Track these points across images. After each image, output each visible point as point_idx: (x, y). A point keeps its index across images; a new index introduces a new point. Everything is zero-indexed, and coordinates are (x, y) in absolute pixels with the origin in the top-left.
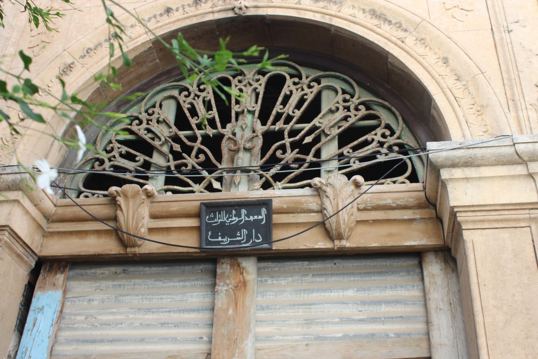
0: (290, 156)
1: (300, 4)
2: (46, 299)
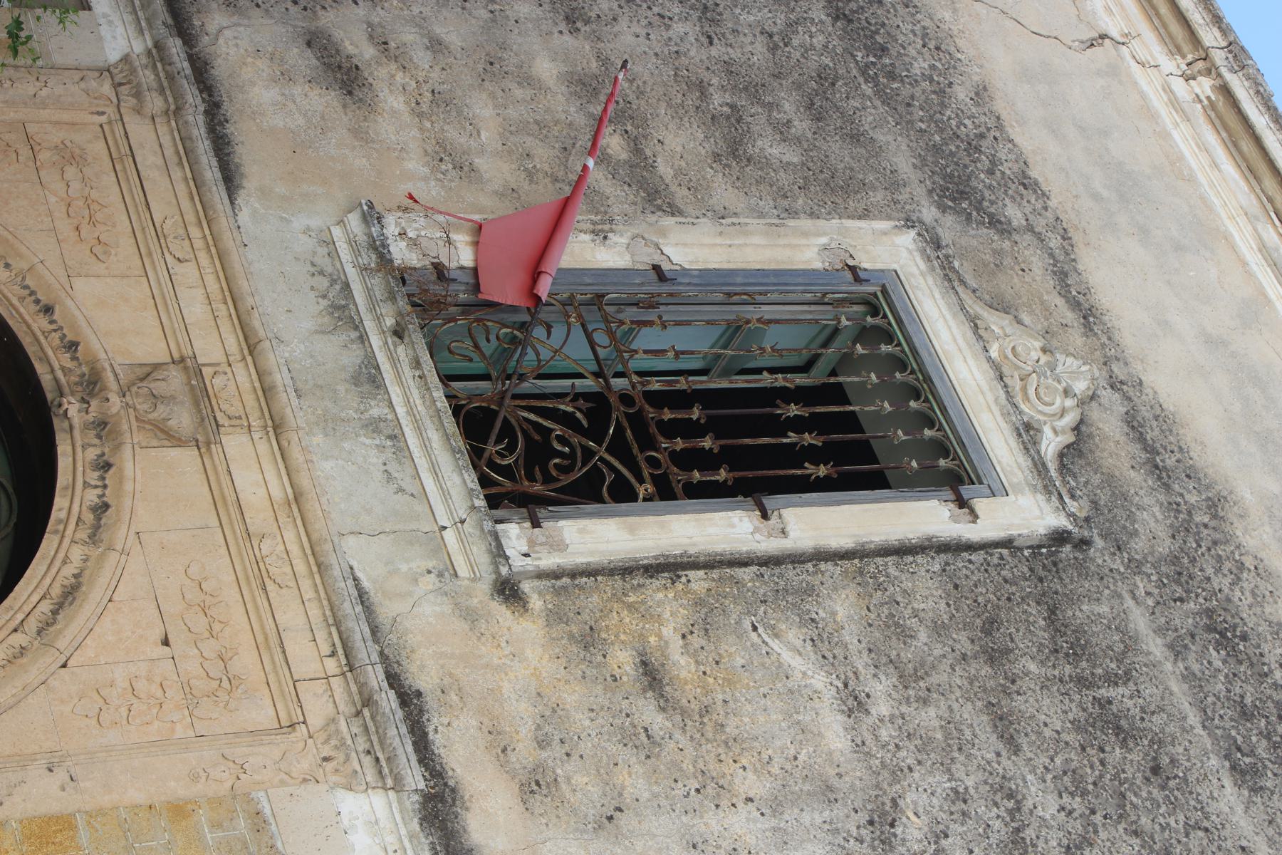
1: (84, 488)
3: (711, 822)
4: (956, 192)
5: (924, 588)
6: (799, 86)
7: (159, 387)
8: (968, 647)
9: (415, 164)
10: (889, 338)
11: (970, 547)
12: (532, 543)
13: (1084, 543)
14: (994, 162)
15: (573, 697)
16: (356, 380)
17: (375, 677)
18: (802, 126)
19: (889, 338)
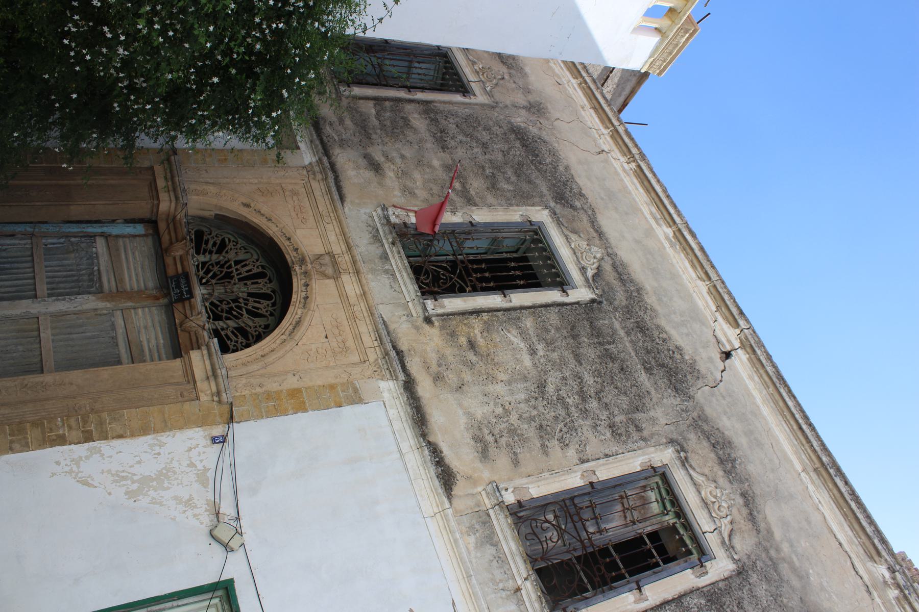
0: (225, 307)
2: (140, 229)
3: (491, 388)
4: (560, 198)
5: (553, 317)
6: (512, 167)
7: (322, 261)
8: (566, 334)
9: (397, 193)
10: (541, 242)
11: (567, 304)
12: (435, 306)
13: (600, 303)
14: (571, 189)
15: (448, 351)
16: (381, 258)
17: (389, 347)
18: (513, 179)
19: (541, 242)
